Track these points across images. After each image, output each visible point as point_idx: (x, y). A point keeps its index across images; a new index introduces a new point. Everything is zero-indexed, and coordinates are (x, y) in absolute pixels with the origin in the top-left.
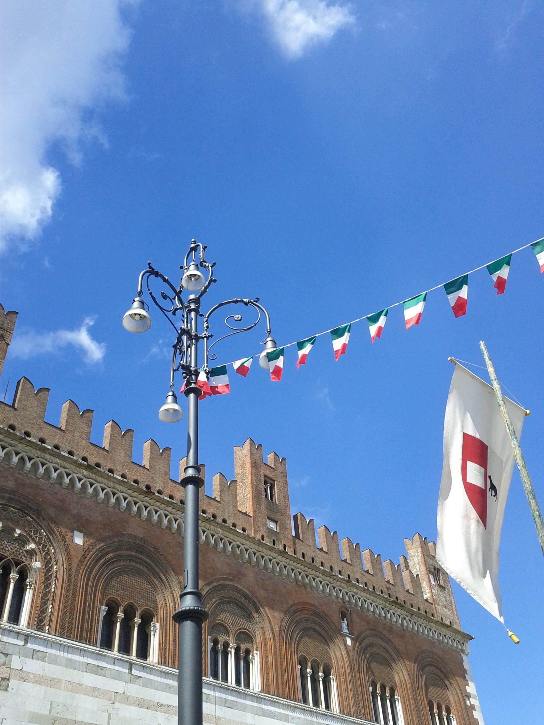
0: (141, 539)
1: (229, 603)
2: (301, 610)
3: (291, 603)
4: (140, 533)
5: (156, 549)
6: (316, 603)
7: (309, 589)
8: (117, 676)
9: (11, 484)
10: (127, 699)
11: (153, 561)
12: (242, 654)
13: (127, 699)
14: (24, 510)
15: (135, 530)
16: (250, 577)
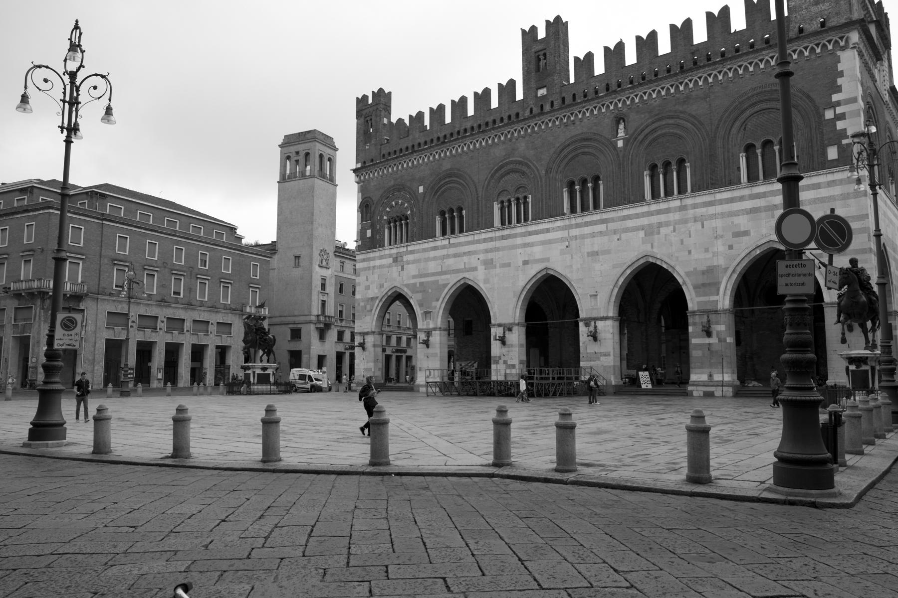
0: (450, 170)
1: (508, 173)
2: (569, 145)
3: (558, 145)
4: (448, 167)
5: (459, 170)
6: (585, 130)
7: (578, 123)
8: (444, 247)
9: (392, 183)
10: (448, 256)
11: (457, 177)
12: (522, 201)
13: (448, 256)
14: (399, 191)
15: (447, 166)
16: (522, 146)
